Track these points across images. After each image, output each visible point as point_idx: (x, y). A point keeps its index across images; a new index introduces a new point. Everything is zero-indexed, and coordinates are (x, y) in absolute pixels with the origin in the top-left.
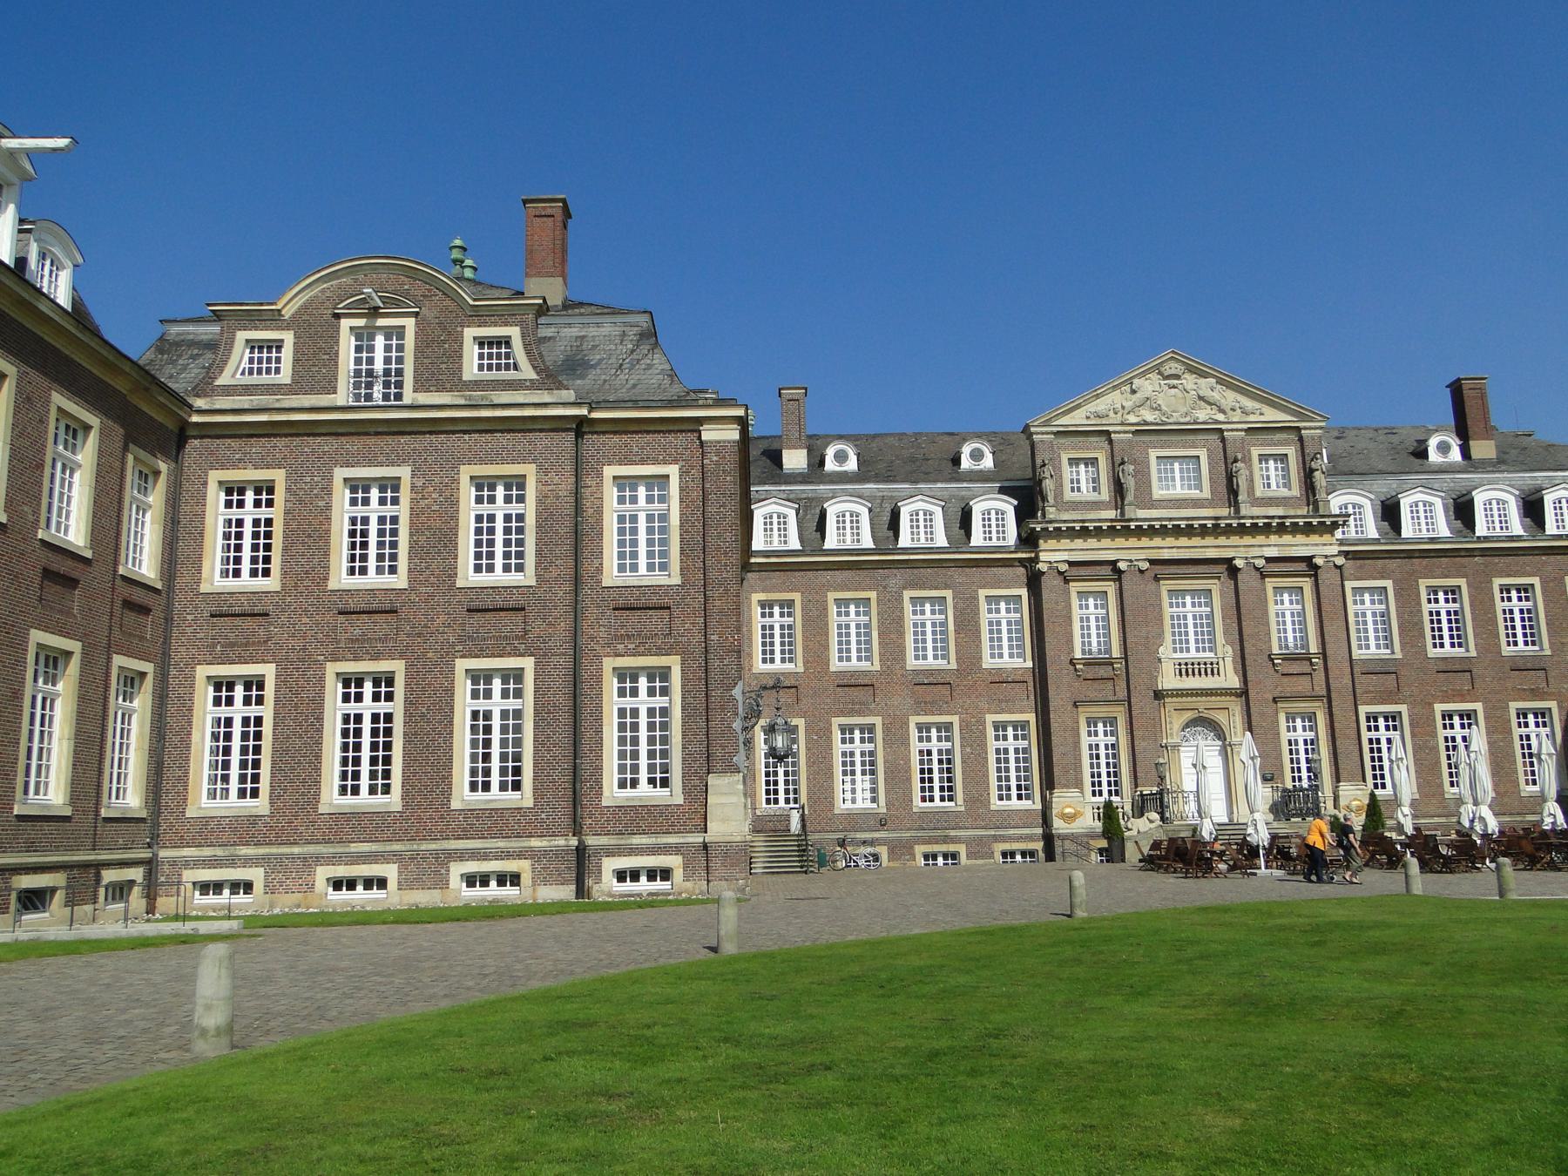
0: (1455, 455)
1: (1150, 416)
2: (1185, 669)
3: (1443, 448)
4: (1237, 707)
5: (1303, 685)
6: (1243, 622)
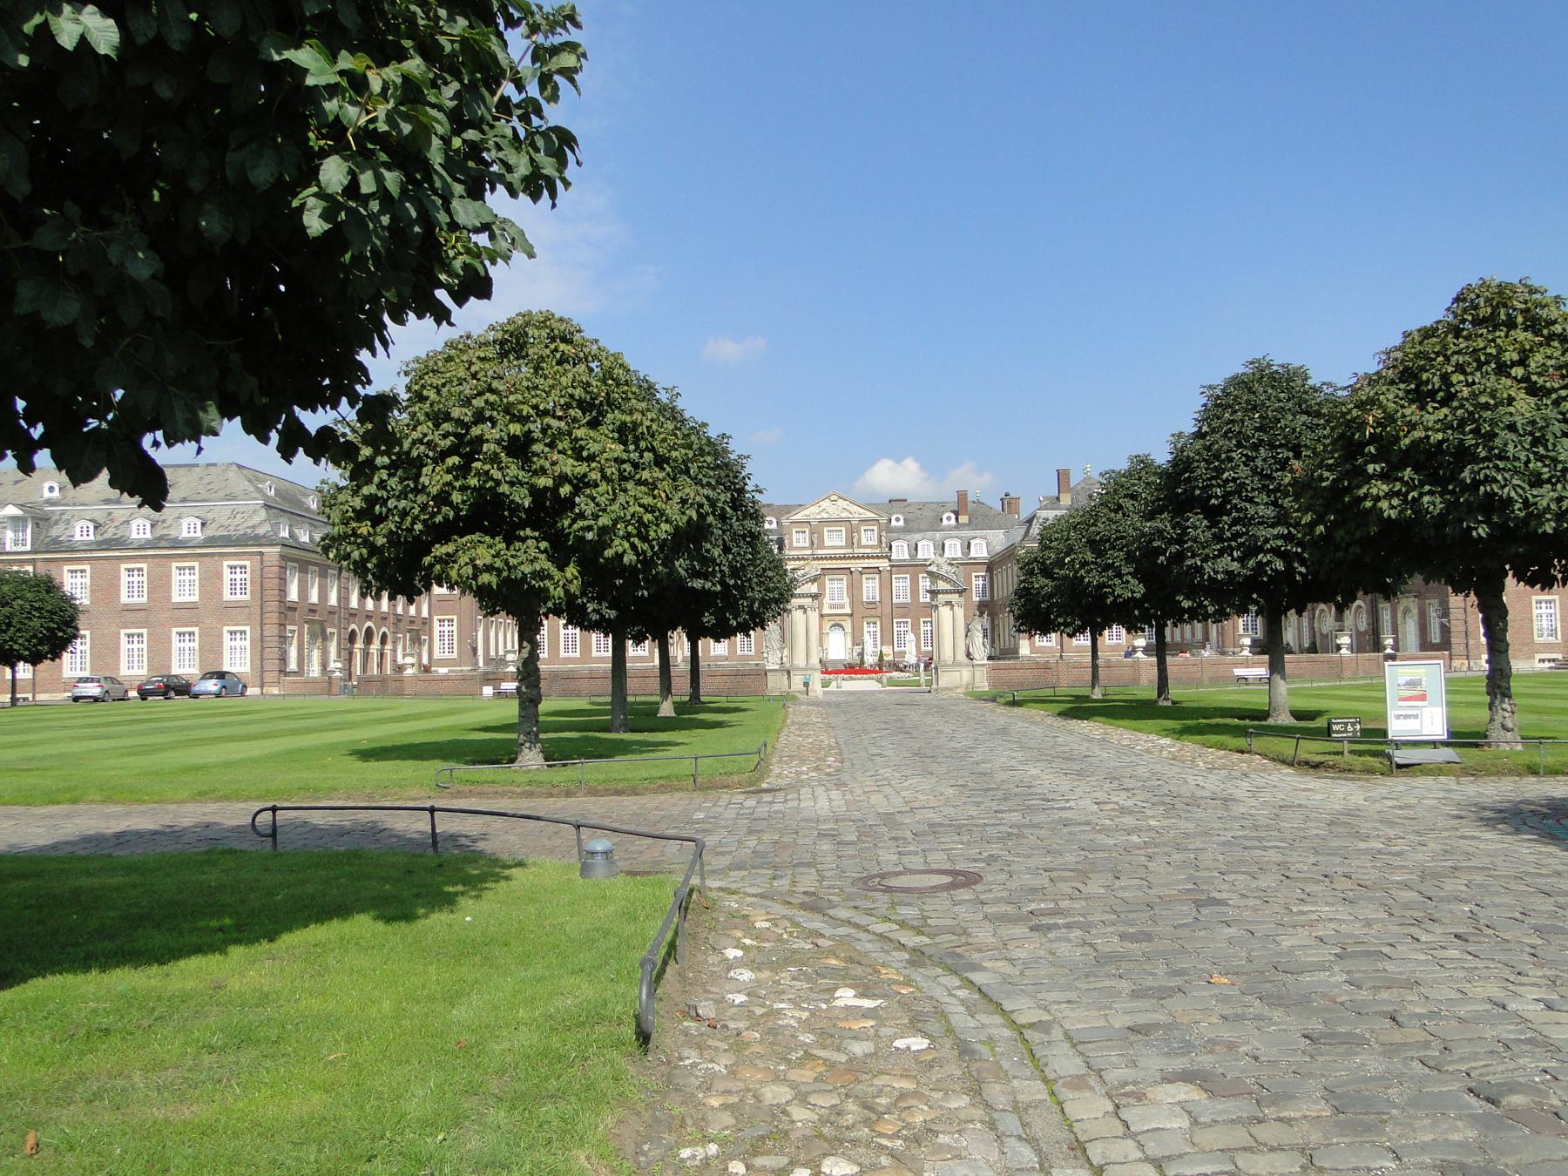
0: (953, 522)
1: (825, 515)
2: (832, 606)
3: (948, 520)
4: (849, 620)
5: (873, 612)
6: (854, 590)
